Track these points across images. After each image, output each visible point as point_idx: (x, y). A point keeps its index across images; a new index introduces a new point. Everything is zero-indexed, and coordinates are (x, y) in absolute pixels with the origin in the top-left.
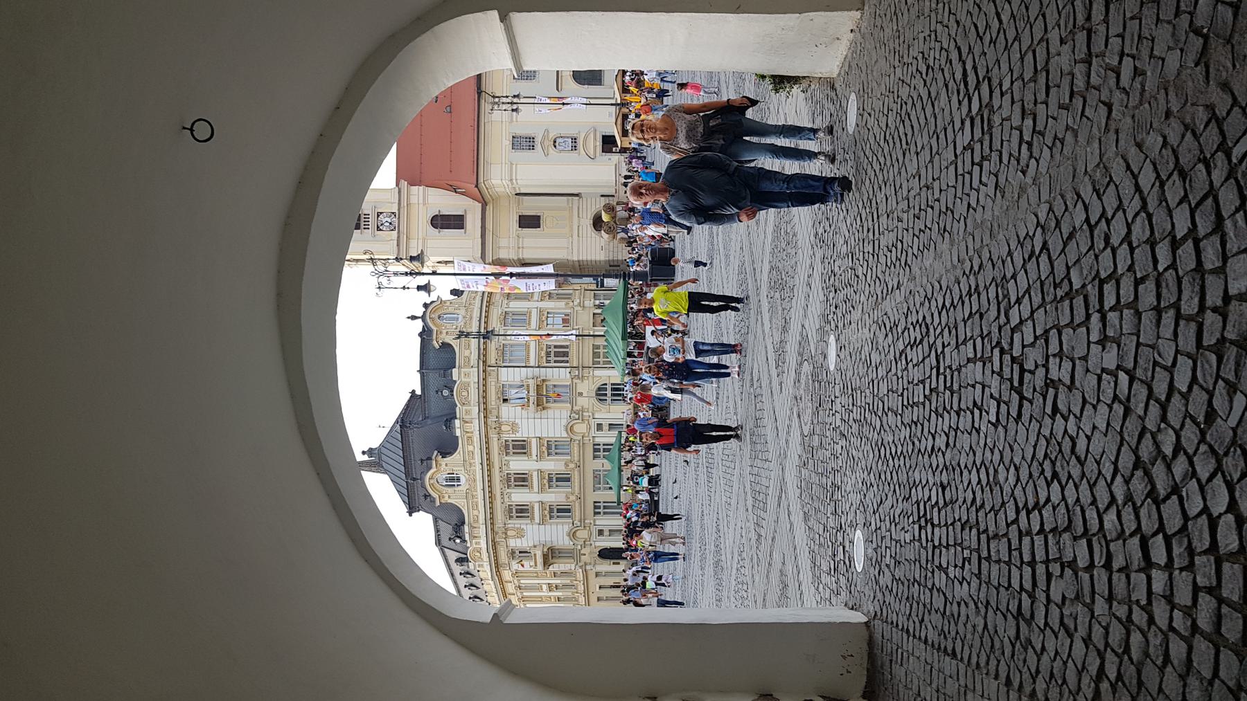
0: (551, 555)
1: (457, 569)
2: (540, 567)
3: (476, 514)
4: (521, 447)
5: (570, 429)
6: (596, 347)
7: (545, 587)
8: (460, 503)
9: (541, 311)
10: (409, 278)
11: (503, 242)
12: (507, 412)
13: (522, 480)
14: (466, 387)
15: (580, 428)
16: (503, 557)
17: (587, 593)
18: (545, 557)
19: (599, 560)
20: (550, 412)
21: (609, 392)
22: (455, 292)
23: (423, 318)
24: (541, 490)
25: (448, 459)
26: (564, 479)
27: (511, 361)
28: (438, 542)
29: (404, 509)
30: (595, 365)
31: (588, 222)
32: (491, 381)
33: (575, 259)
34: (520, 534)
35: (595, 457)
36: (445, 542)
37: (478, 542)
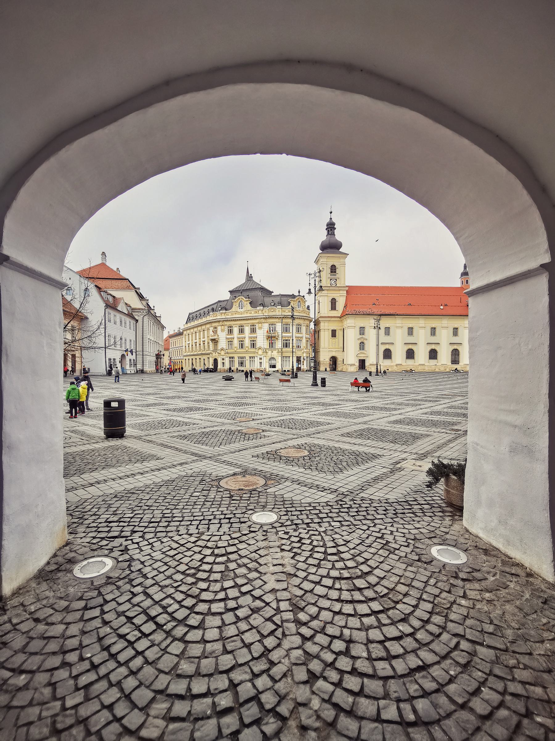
0: (215, 341)
1: (210, 308)
2: (211, 338)
3: (229, 315)
4: (253, 331)
7: (204, 339)
8: (233, 309)
9: (302, 337)
10: (314, 286)
11: (326, 324)
12: (266, 326)
13: (242, 331)
15: (260, 352)
16: (214, 325)
17: (202, 354)
18: (214, 340)
19: (213, 359)
22: (308, 307)
23: (299, 295)
24: (238, 338)
25: (249, 305)
26: (242, 346)
28: (219, 301)
29: (231, 289)
30: (283, 357)
31: (334, 354)
32: (277, 320)
34: (223, 331)
36: (219, 304)
37: (219, 315)
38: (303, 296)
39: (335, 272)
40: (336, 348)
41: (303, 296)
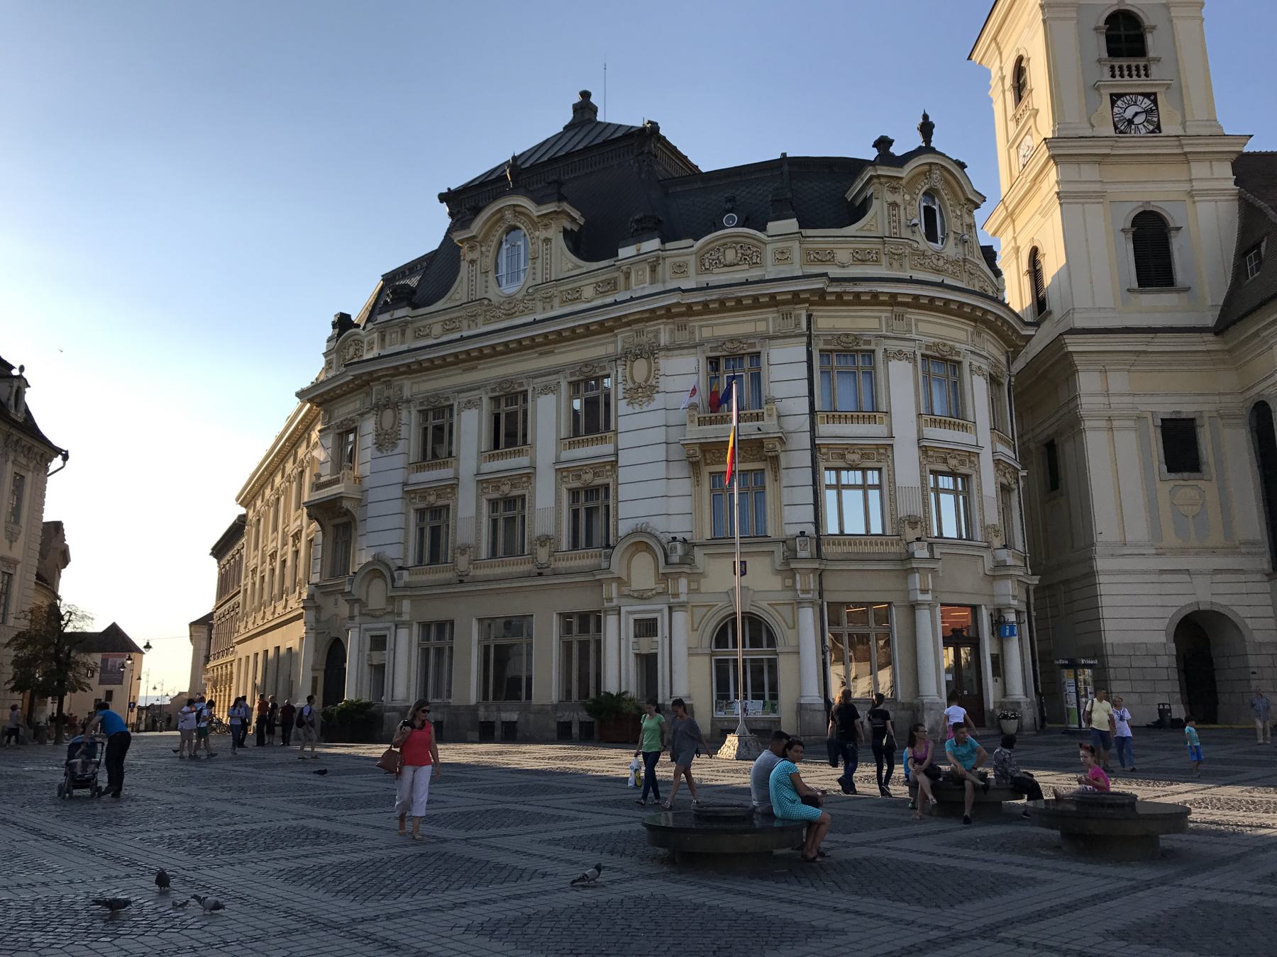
5: (642, 541)
8: (460, 292)
9: (971, 456)
11: (1119, 381)
12: (682, 374)
14: (749, 256)
15: (643, 573)
20: (685, 486)
25: (559, 242)
27: (825, 373)
31: (1203, 594)
33: (1100, 564)
35: (565, 617)
39: (1141, 51)
40: (1213, 551)
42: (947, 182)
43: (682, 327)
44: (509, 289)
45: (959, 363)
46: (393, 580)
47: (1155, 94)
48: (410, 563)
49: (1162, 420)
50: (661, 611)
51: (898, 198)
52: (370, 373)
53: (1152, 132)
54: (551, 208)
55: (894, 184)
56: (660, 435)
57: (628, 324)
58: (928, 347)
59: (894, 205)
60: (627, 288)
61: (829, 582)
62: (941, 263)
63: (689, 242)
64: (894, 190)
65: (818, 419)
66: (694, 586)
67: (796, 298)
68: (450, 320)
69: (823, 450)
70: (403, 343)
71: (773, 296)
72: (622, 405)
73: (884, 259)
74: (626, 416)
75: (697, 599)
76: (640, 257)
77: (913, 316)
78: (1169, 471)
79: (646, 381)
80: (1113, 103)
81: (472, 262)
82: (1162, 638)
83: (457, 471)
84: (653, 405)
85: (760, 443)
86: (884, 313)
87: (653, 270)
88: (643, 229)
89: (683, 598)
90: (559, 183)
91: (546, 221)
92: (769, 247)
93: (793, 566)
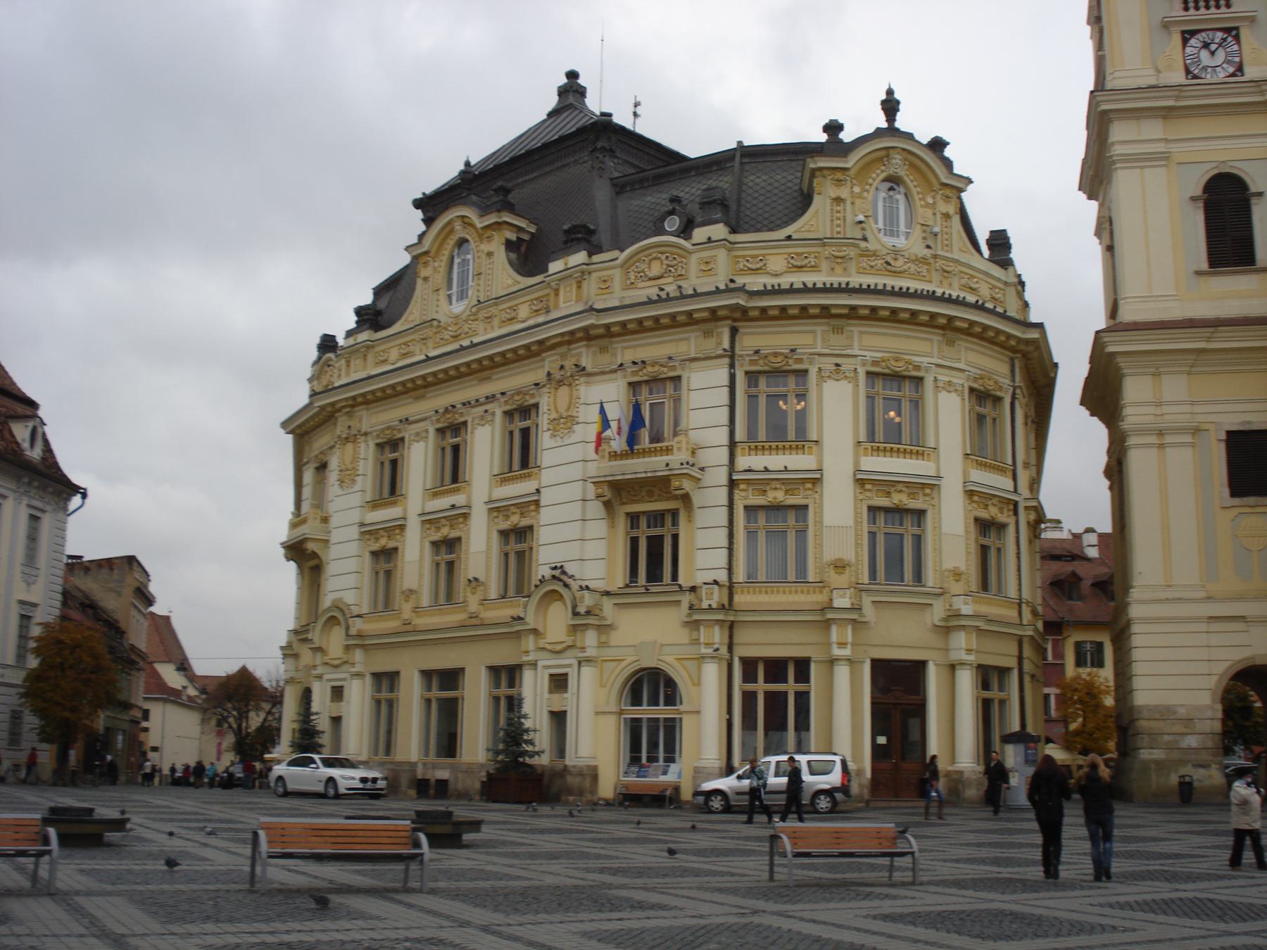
4: (522, 454)
6: (802, 666)
9: (929, 487)
11: (1175, 386)
15: (556, 622)
20: (599, 528)
21: (662, 712)
25: (501, 255)
32: (688, 343)
35: (495, 671)
38: (938, 145)
41: (938, 145)
42: (912, 166)
43: (603, 350)
44: (458, 308)
45: (921, 379)
46: (347, 628)
47: (1237, 29)
48: (365, 610)
49: (1229, 433)
50: (569, 666)
51: (844, 192)
52: (333, 404)
53: (1233, 75)
54: (492, 219)
55: (839, 175)
56: (576, 471)
57: (553, 347)
58: (875, 363)
59: (838, 200)
60: (557, 307)
61: (740, 636)
62: (900, 263)
63: (615, 253)
64: (839, 182)
65: (738, 451)
66: (604, 639)
67: (714, 314)
68: (405, 344)
69: (742, 486)
70: (365, 369)
71: (689, 314)
72: (547, 435)
73: (825, 265)
74: (548, 449)
75: (608, 653)
76: (565, 275)
77: (855, 329)
78: (1233, 495)
79: (568, 409)
80: (1185, 42)
81: (426, 279)
82: (1205, 699)
83: (405, 510)
84: (574, 438)
85: (666, 480)
86: (820, 328)
87: (579, 287)
88: (572, 240)
89: (590, 652)
90: (507, 191)
91: (489, 233)
92: (694, 258)
93: (696, 617)
